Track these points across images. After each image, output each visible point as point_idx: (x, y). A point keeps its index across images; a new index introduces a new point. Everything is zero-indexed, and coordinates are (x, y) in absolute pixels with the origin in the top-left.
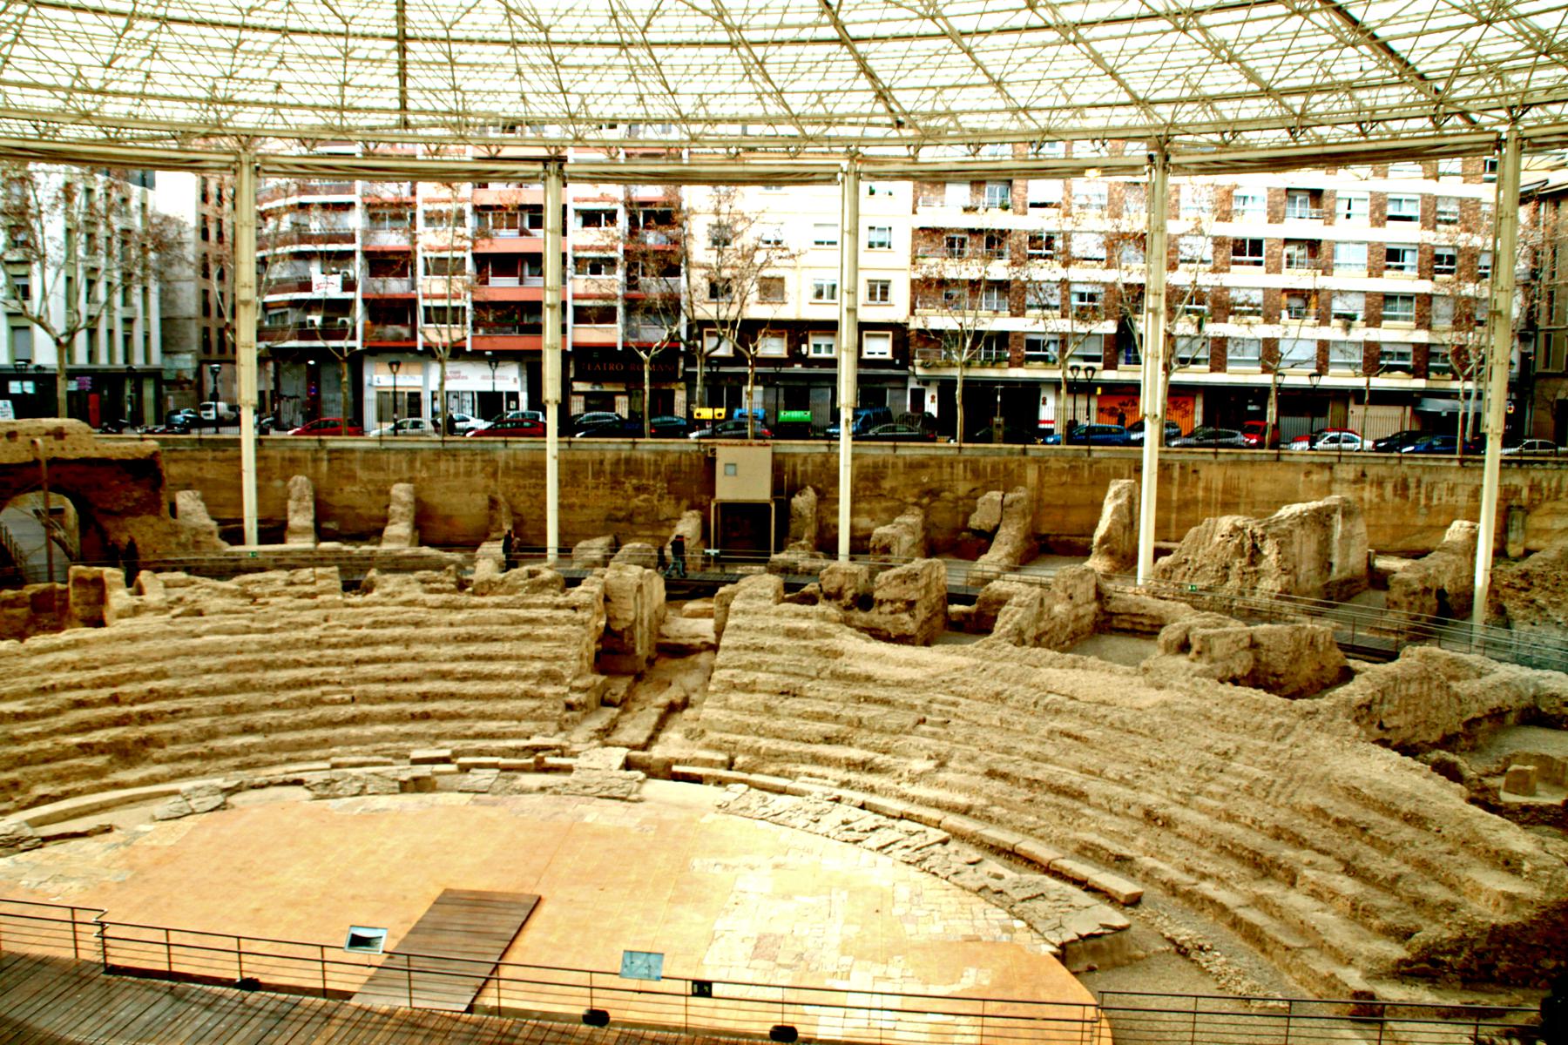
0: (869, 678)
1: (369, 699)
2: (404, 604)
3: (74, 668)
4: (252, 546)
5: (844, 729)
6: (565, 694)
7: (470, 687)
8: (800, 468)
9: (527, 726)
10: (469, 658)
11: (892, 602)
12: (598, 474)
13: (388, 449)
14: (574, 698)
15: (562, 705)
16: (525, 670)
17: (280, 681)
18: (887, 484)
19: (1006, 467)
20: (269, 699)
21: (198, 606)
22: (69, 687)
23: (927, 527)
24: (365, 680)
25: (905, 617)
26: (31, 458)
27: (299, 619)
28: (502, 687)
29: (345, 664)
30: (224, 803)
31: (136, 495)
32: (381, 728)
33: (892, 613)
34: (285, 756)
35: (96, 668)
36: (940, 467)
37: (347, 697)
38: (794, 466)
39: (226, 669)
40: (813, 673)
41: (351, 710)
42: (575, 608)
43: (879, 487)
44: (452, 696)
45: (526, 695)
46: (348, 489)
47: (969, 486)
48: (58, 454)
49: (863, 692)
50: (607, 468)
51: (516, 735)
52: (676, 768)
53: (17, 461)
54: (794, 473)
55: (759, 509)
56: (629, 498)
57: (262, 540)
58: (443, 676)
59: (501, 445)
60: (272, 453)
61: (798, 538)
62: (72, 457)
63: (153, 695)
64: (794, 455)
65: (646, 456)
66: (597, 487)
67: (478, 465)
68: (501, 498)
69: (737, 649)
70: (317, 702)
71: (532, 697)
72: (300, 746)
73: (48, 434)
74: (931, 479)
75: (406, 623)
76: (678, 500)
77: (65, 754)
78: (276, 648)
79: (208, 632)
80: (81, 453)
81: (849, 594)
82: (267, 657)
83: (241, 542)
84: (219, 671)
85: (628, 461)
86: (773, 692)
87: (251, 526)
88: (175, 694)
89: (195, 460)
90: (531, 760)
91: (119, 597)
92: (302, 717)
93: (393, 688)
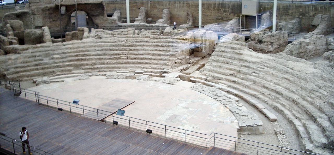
0: (246, 61)
1: (132, 59)
2: (145, 37)
3: (71, 49)
4: (128, 23)
5: (235, 72)
7: (153, 57)
8: (266, 7)
9: (164, 67)
10: (155, 50)
11: (267, 42)
12: (214, 7)
14: (176, 61)
16: (167, 54)
17: (112, 54)
18: (290, 12)
19: (325, 7)
20: (109, 57)
21: (101, 36)
23: (300, 23)
24: (131, 54)
25: (270, 46)
27: (120, 40)
28: (162, 57)
29: (128, 50)
30: (88, 78)
31: (98, 11)
32: (131, 65)
33: (267, 45)
34: (109, 70)
35: (75, 49)
36: (306, 7)
37: (126, 58)
38: (265, 6)
39: (102, 50)
40: (234, 58)
41: (126, 61)
42: (184, 40)
43: (287, 12)
45: (166, 60)
46: (155, 10)
47: (314, 13)
49: (243, 64)
51: (160, 69)
52: (191, 79)
53: (72, 4)
55: (253, 17)
56: (222, 14)
57: (130, 22)
58: (149, 54)
61: (263, 25)
62: (83, 3)
63: (84, 55)
65: (226, 3)
66: (214, 11)
67: (185, 5)
68: (190, 13)
69: (218, 51)
70: (119, 58)
72: (113, 68)
74: (303, 10)
75: (144, 42)
76: (234, 15)
77: (65, 66)
78: (114, 46)
79: (100, 42)
81: (257, 39)
82: (111, 48)
83: (126, 22)
84: (100, 51)
85: (222, 4)
86: (222, 62)
87: (128, 19)
88: (89, 55)
90: (159, 74)
91: (86, 34)
92: (115, 62)
93: (136, 56)
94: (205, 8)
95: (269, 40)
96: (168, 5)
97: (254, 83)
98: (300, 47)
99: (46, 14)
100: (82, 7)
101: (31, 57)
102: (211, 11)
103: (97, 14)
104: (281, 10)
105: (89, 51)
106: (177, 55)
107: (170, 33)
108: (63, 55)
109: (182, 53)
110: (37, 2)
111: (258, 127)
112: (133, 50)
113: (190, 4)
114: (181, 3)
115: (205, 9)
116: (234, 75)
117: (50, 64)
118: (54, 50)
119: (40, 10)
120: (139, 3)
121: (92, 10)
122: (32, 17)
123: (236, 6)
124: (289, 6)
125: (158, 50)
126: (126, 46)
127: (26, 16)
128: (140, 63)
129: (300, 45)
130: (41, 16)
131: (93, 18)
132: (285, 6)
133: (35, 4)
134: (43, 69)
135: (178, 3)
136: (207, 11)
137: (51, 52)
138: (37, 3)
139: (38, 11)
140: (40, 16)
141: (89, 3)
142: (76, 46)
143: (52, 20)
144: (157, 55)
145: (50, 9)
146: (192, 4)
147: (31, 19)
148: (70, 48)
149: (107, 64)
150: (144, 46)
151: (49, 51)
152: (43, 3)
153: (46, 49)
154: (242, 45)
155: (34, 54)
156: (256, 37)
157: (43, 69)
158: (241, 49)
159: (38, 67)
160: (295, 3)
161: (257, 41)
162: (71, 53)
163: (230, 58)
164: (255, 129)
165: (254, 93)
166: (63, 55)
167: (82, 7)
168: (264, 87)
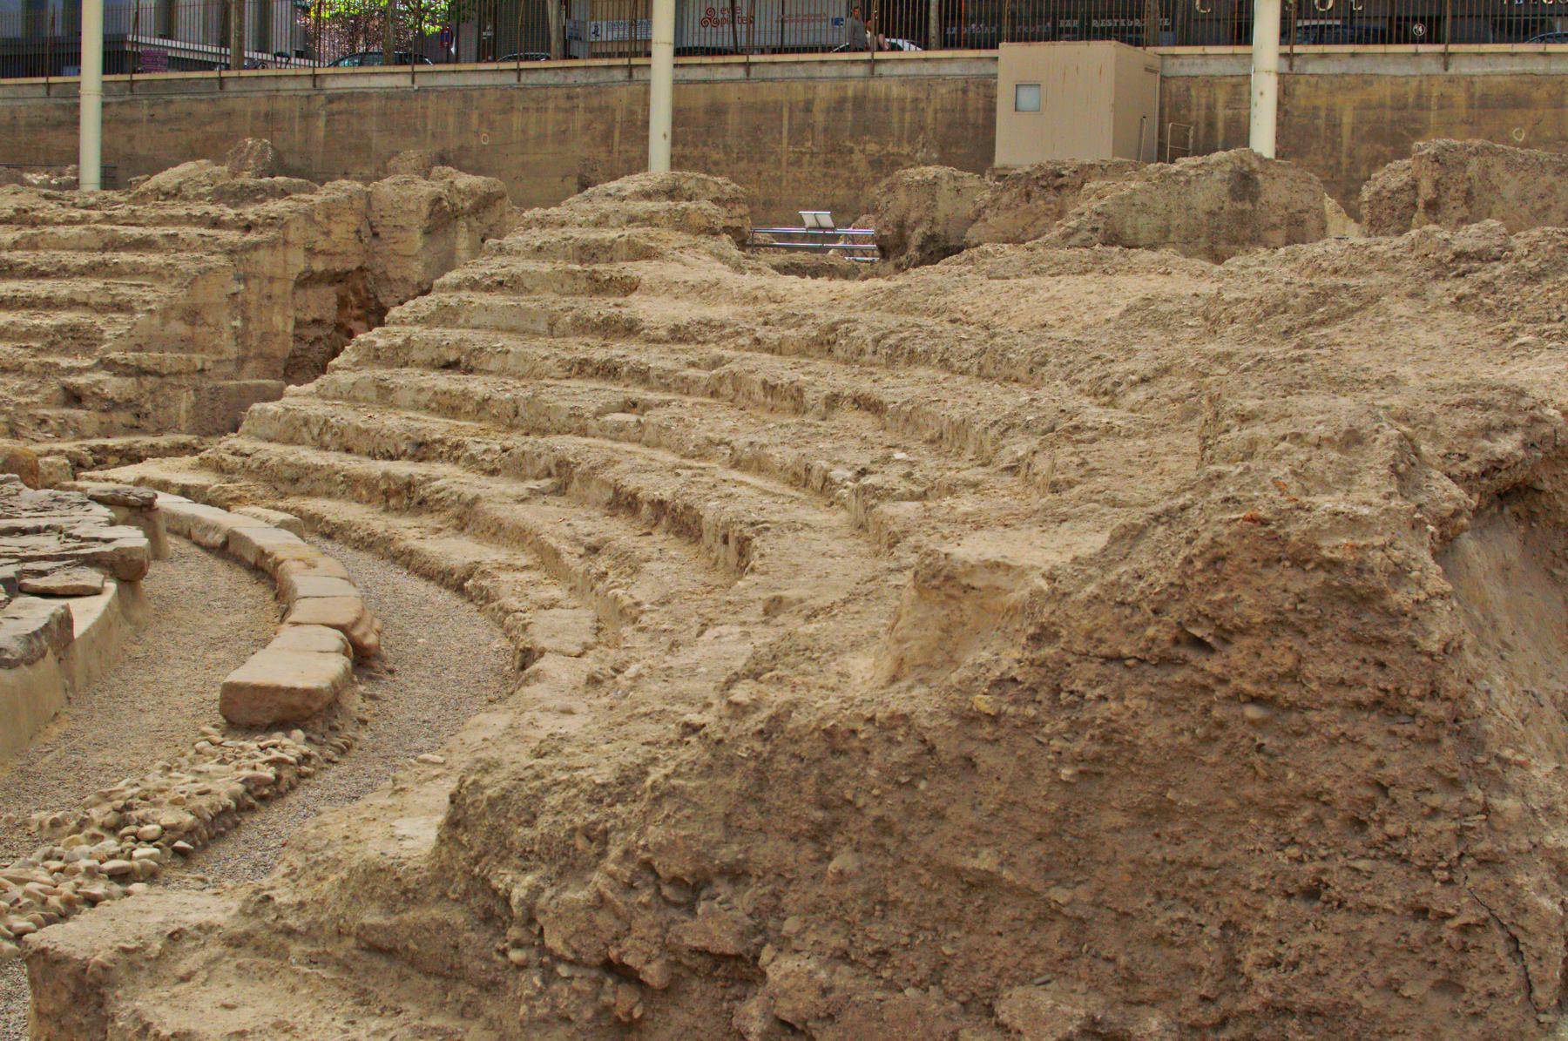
0: (630, 329)
6: (71, 371)
8: (1222, 113)
12: (797, 136)
13: (425, 90)
14: (81, 380)
15: (54, 385)
38: (1211, 108)
40: (542, 326)
50: (819, 118)
54: (1211, 124)
59: (620, 75)
60: (239, 104)
64: (1209, 82)
65: (896, 91)
66: (798, 162)
67: (580, 118)
81: (916, 238)
85: (860, 102)
89: (123, 121)
94: (729, 141)
95: (1020, 223)
96: (451, 129)
97: (560, 490)
98: (1241, 218)
102: (779, 162)
104: (1346, 131)
107: (179, 189)
109: (179, 328)
113: (618, 118)
114: (551, 105)
115: (727, 150)
116: (457, 446)
123: (971, 116)
124: (1419, 96)
129: (1235, 195)
132: (1382, 106)
135: (526, 109)
136: (743, 165)
146: (632, 112)
154: (681, 223)
156: (913, 215)
158: (646, 254)
160: (1465, 70)
161: (921, 248)
163: (512, 330)
165: (457, 550)
168: (624, 503)
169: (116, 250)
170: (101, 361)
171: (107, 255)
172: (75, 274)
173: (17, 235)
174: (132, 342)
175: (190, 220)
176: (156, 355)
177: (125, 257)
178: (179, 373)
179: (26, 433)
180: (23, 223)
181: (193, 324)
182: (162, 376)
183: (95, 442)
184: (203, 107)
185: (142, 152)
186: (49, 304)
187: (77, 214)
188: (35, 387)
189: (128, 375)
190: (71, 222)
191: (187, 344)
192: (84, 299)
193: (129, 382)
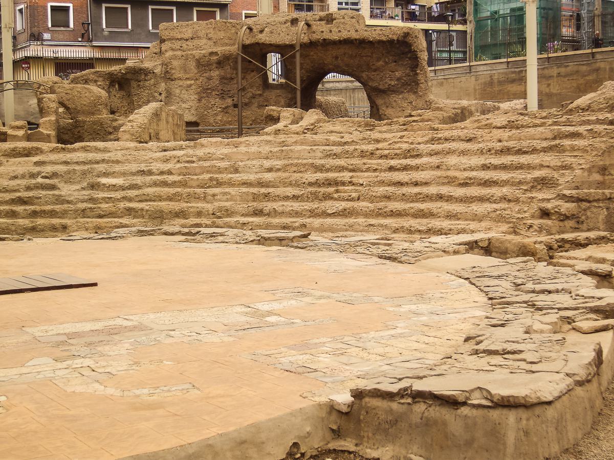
1: (372, 199)
6: (543, 200)
7: (460, 192)
10: (485, 167)
14: (549, 206)
15: (535, 207)
20: (290, 191)
22: (162, 173)
24: (382, 183)
26: (305, 39)
37: (354, 195)
39: (284, 169)
44: (440, 197)
45: (504, 199)
48: (327, 36)
58: (451, 181)
60: (602, 65)
62: (335, 36)
71: (509, 201)
73: (321, 20)
80: (345, 35)
82: (319, 162)
99: (209, 79)
100: (337, 58)
101: (23, 177)
103: (393, 83)
105: (236, 171)
106: (562, 181)
107: (589, 107)
108: (139, 180)
109: (597, 177)
110: (186, 36)
111: (495, 414)
112: (398, 170)
117: (68, 202)
118: (118, 162)
119: (192, 65)
120: (608, 70)
121: (375, 70)
122: (162, 86)
125: (496, 167)
126: (381, 157)
127: (141, 83)
128: (393, 214)
130: (193, 87)
131: (379, 101)
133: (177, 45)
134: (35, 214)
137: (101, 167)
138: (187, 40)
139: (185, 69)
140: (191, 85)
141: (358, 37)
142: (200, 152)
143: (229, 101)
144: (480, 184)
145: (223, 61)
147: (160, 94)
148: (177, 159)
149: (274, 213)
150: (450, 152)
151: (97, 162)
152: (204, 41)
153: (91, 156)
155: (37, 169)
157: (35, 214)
159: (19, 208)
162: (170, 173)
164: (470, 425)
166: (139, 180)
167: (337, 58)
169: (561, 138)
170: (559, 195)
171: (557, 142)
172: (541, 151)
173: (510, 134)
174: (574, 185)
175: (598, 121)
176: (586, 191)
177: (567, 142)
178: (598, 200)
179: (522, 232)
180: (512, 127)
181: (604, 175)
182: (589, 202)
183: (557, 237)
184: (584, 68)
185: (555, 92)
186: (530, 167)
187: (538, 121)
188: (526, 209)
189: (573, 202)
190: (536, 126)
191: (601, 185)
192: (548, 164)
193: (571, 206)
